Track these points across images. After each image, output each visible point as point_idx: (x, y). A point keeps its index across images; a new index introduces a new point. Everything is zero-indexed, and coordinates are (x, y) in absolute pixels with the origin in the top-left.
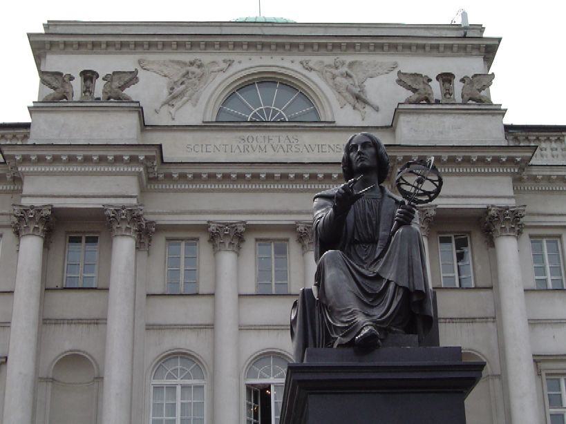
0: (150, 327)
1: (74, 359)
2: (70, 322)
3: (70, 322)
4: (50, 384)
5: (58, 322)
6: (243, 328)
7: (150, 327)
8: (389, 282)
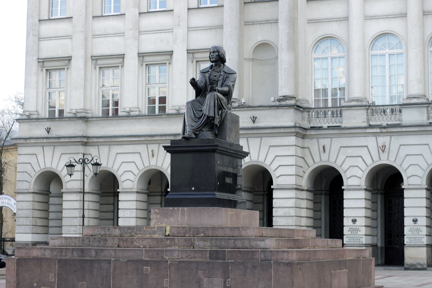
0: (311, 21)
1: (264, 46)
2: (260, 23)
3: (260, 23)
4: (251, 62)
5: (253, 23)
6: (368, 18)
7: (311, 21)
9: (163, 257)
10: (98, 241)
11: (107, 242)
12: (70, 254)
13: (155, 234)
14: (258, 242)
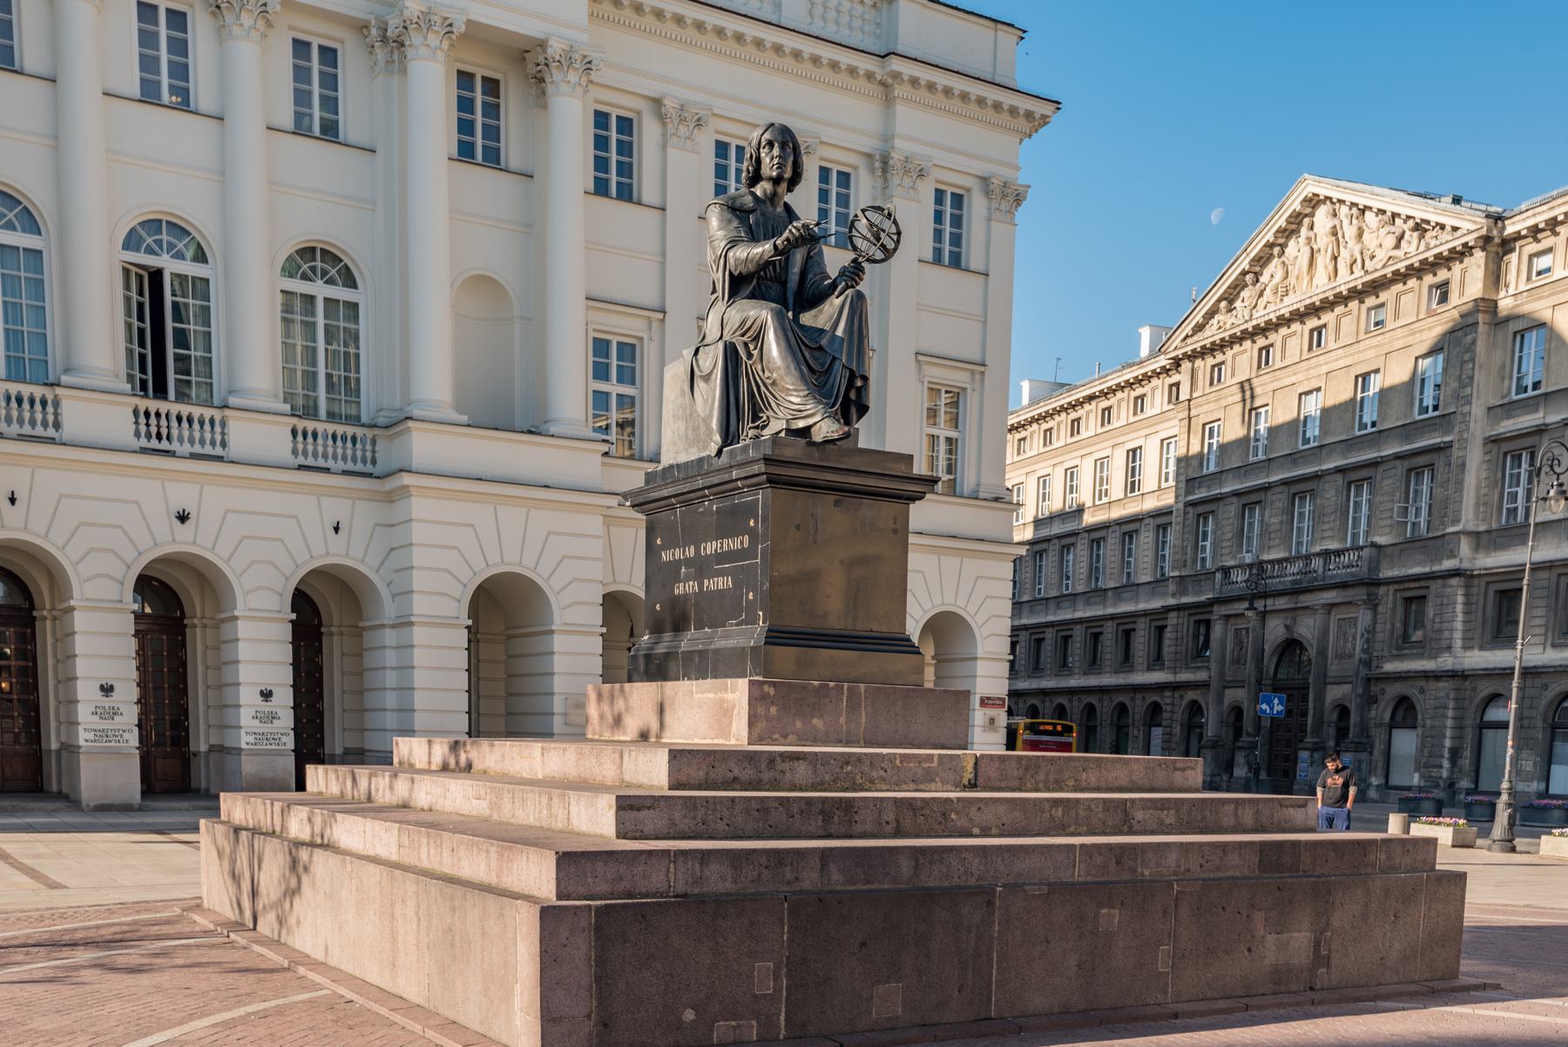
8: (834, 358)
9: (1134, 870)
10: (822, 812)
11: (857, 818)
12: (815, 875)
13: (933, 780)
14: (1291, 811)
